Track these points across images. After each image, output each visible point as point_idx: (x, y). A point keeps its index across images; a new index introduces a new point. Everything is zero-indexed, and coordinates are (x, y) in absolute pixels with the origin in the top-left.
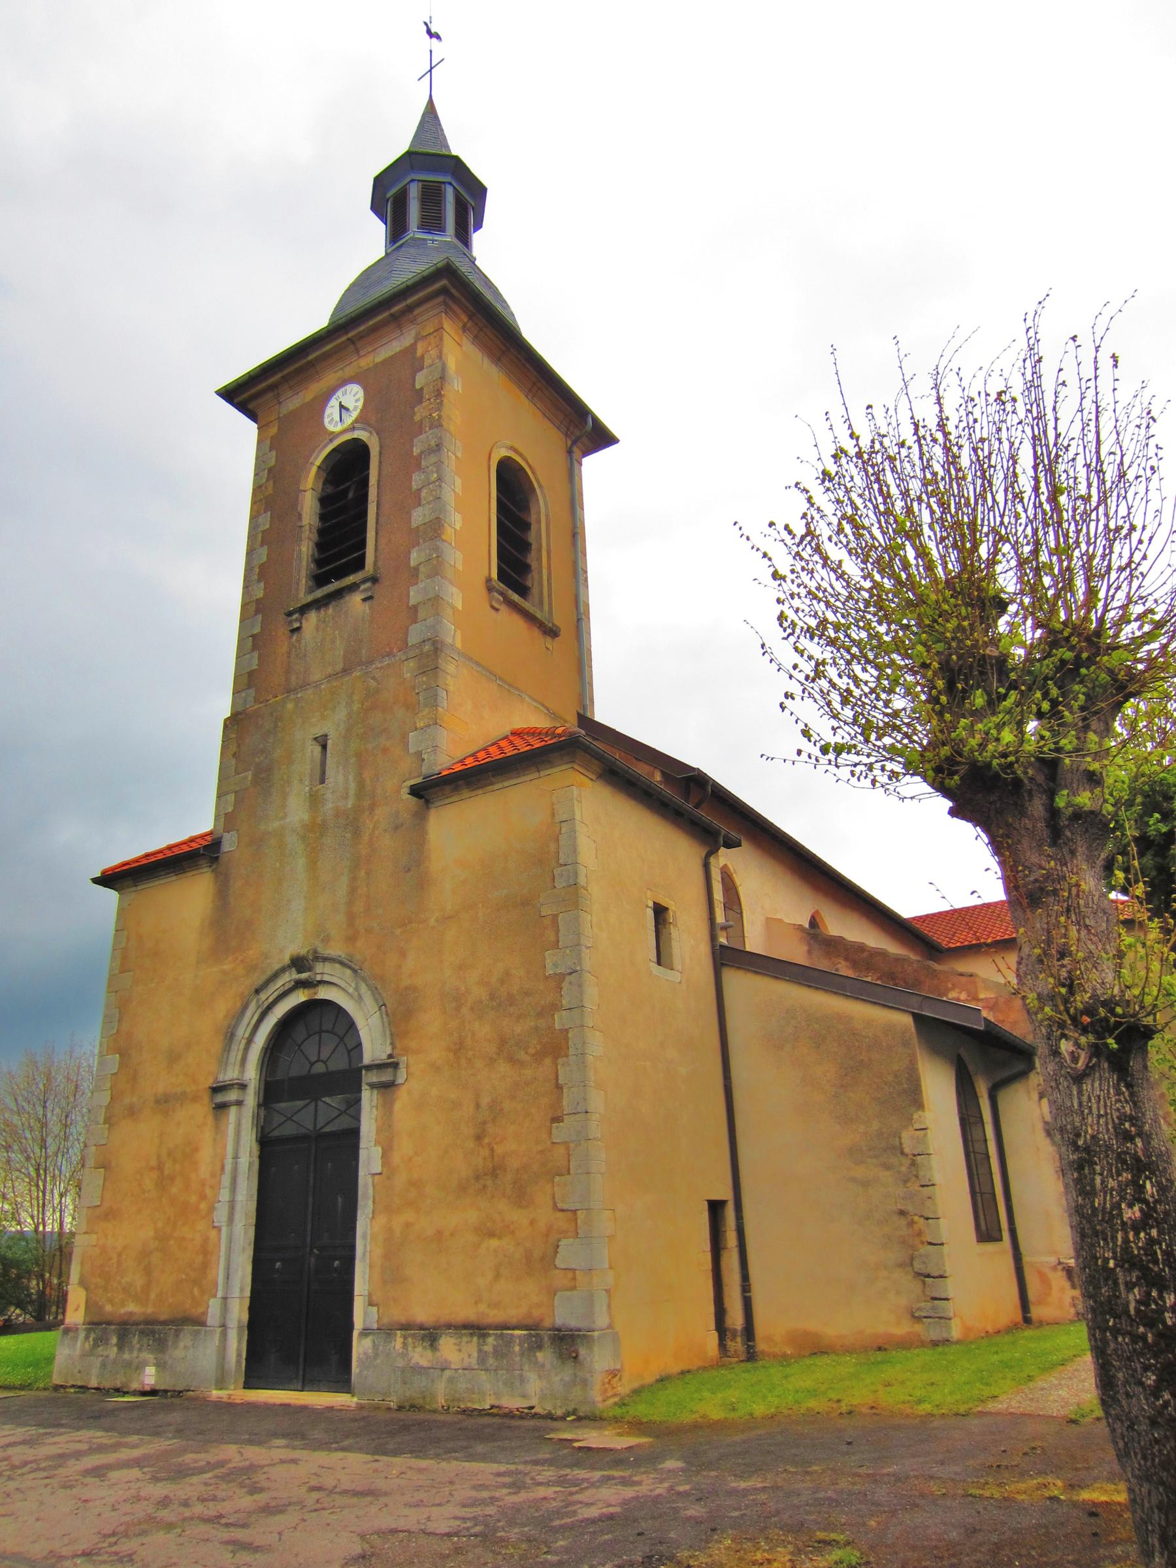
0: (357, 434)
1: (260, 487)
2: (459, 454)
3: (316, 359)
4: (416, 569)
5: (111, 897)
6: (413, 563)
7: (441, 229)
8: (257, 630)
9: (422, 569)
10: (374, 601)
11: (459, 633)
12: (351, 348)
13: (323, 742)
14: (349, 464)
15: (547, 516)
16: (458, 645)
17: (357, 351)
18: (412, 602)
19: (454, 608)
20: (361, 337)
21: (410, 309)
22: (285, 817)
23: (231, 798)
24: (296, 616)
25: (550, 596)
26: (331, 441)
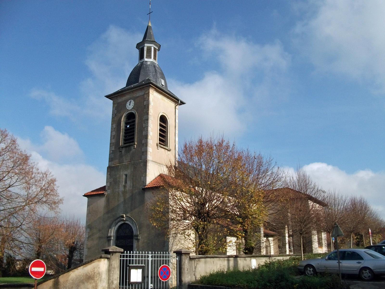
0: (133, 111)
1: (113, 118)
2: (152, 119)
3: (125, 93)
4: (144, 144)
5: (86, 199)
6: (143, 143)
7: (151, 58)
8: (113, 149)
9: (144, 144)
10: (142, 187)
11: (151, 157)
12: (132, 92)
13: (126, 175)
14: (131, 117)
15: (170, 125)
16: (151, 143)
17: (133, 93)
18: (143, 151)
19: (150, 152)
20: (134, 91)
21: (144, 87)
22: (119, 189)
23: (109, 183)
24: (121, 149)
25: (170, 129)
26: (128, 111)
